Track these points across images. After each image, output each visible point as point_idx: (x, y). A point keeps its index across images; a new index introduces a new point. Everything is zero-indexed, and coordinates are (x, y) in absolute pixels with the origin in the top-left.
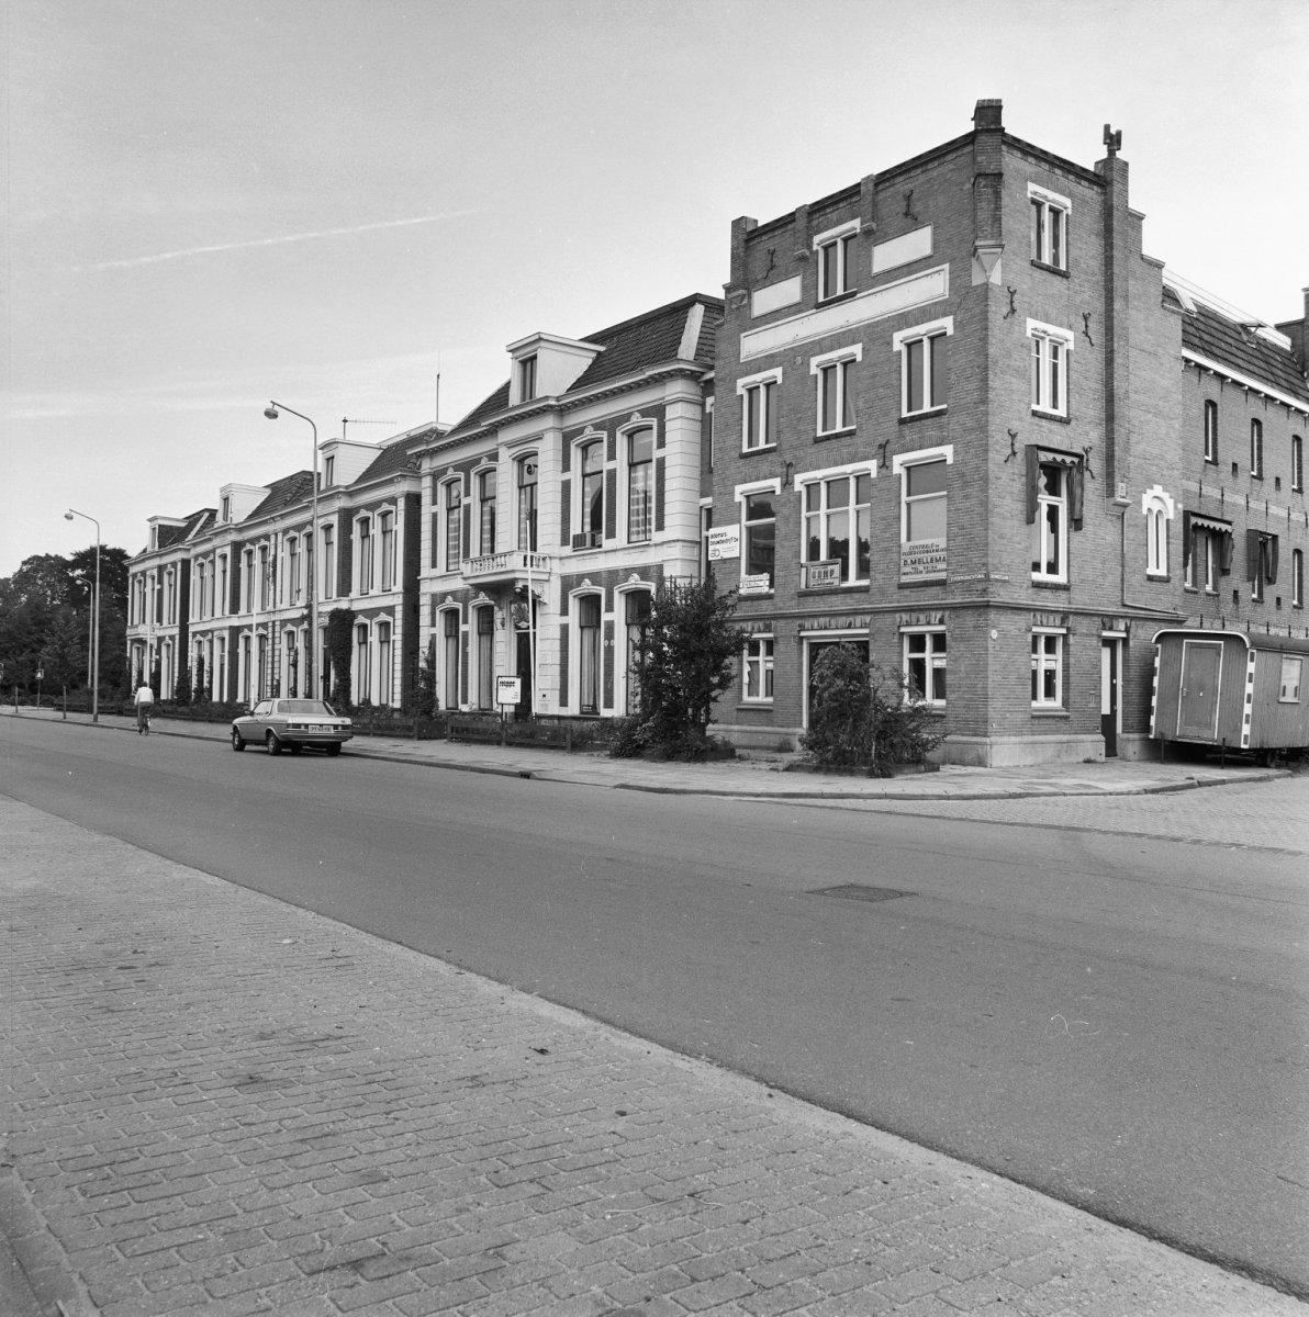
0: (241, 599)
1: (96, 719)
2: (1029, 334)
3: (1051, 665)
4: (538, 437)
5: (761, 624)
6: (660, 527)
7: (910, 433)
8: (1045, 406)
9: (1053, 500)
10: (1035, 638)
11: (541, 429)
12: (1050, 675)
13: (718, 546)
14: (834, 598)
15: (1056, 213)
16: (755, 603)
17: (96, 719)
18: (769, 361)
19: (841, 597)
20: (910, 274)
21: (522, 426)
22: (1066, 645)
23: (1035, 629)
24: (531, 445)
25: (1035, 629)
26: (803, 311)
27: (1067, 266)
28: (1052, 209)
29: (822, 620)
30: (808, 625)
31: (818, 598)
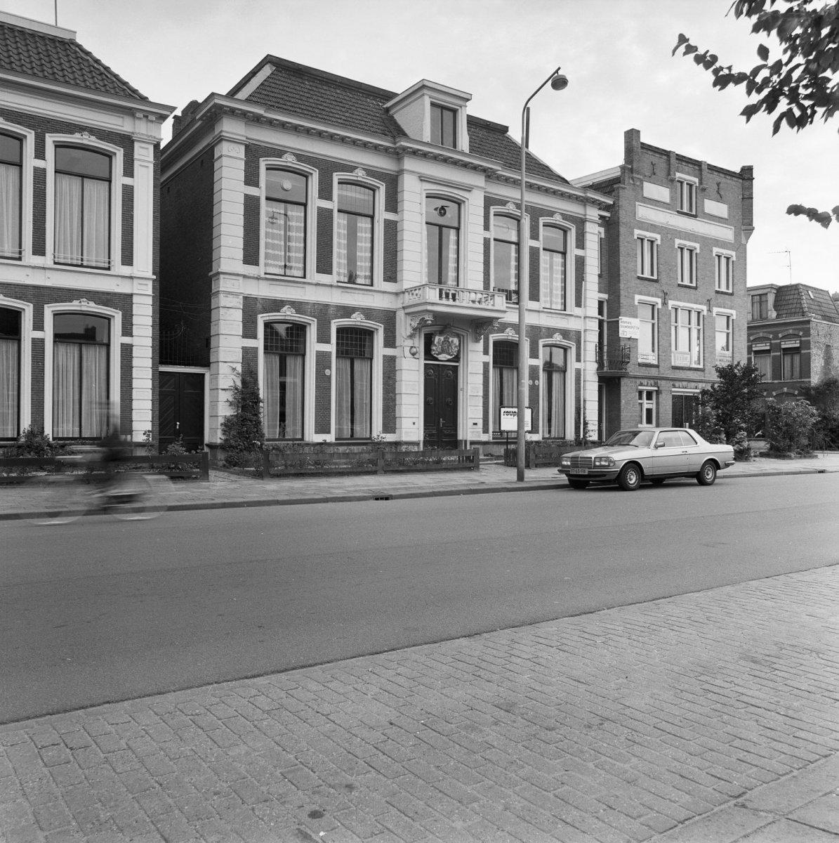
0: (48, 283)
1: (521, 477)
2: (714, 255)
3: (649, 406)
4: (468, 189)
5: (652, 382)
6: (535, 296)
7: (721, 298)
8: (723, 289)
9: (40, 163)
10: (640, 393)
11: (476, 184)
12: (649, 411)
13: (626, 329)
14: (688, 372)
15: (691, 186)
16: (648, 368)
17: (521, 477)
18: (653, 227)
19: (692, 372)
20: (719, 222)
21: (430, 164)
22: (657, 398)
23: (640, 388)
24: (461, 193)
25: (640, 388)
26: (669, 209)
27: (696, 212)
28: (687, 184)
29: (684, 383)
30: (677, 384)
31: (681, 371)
